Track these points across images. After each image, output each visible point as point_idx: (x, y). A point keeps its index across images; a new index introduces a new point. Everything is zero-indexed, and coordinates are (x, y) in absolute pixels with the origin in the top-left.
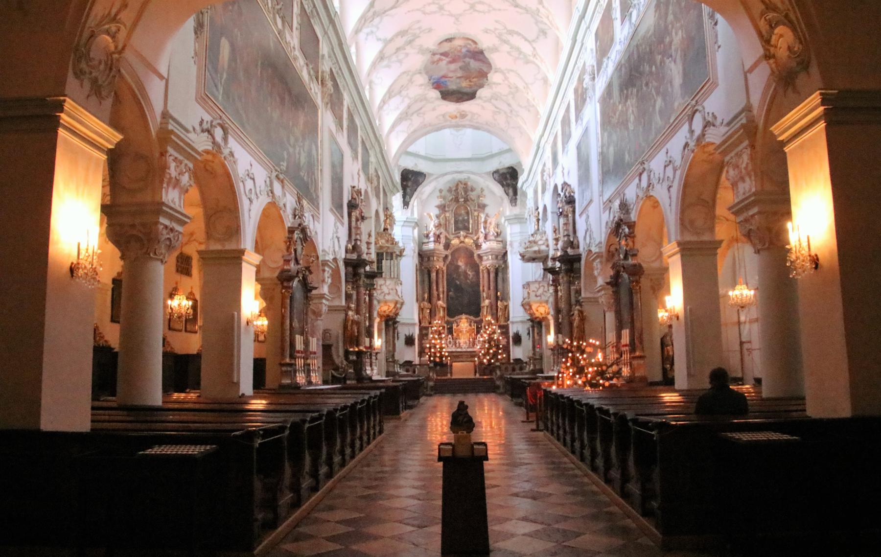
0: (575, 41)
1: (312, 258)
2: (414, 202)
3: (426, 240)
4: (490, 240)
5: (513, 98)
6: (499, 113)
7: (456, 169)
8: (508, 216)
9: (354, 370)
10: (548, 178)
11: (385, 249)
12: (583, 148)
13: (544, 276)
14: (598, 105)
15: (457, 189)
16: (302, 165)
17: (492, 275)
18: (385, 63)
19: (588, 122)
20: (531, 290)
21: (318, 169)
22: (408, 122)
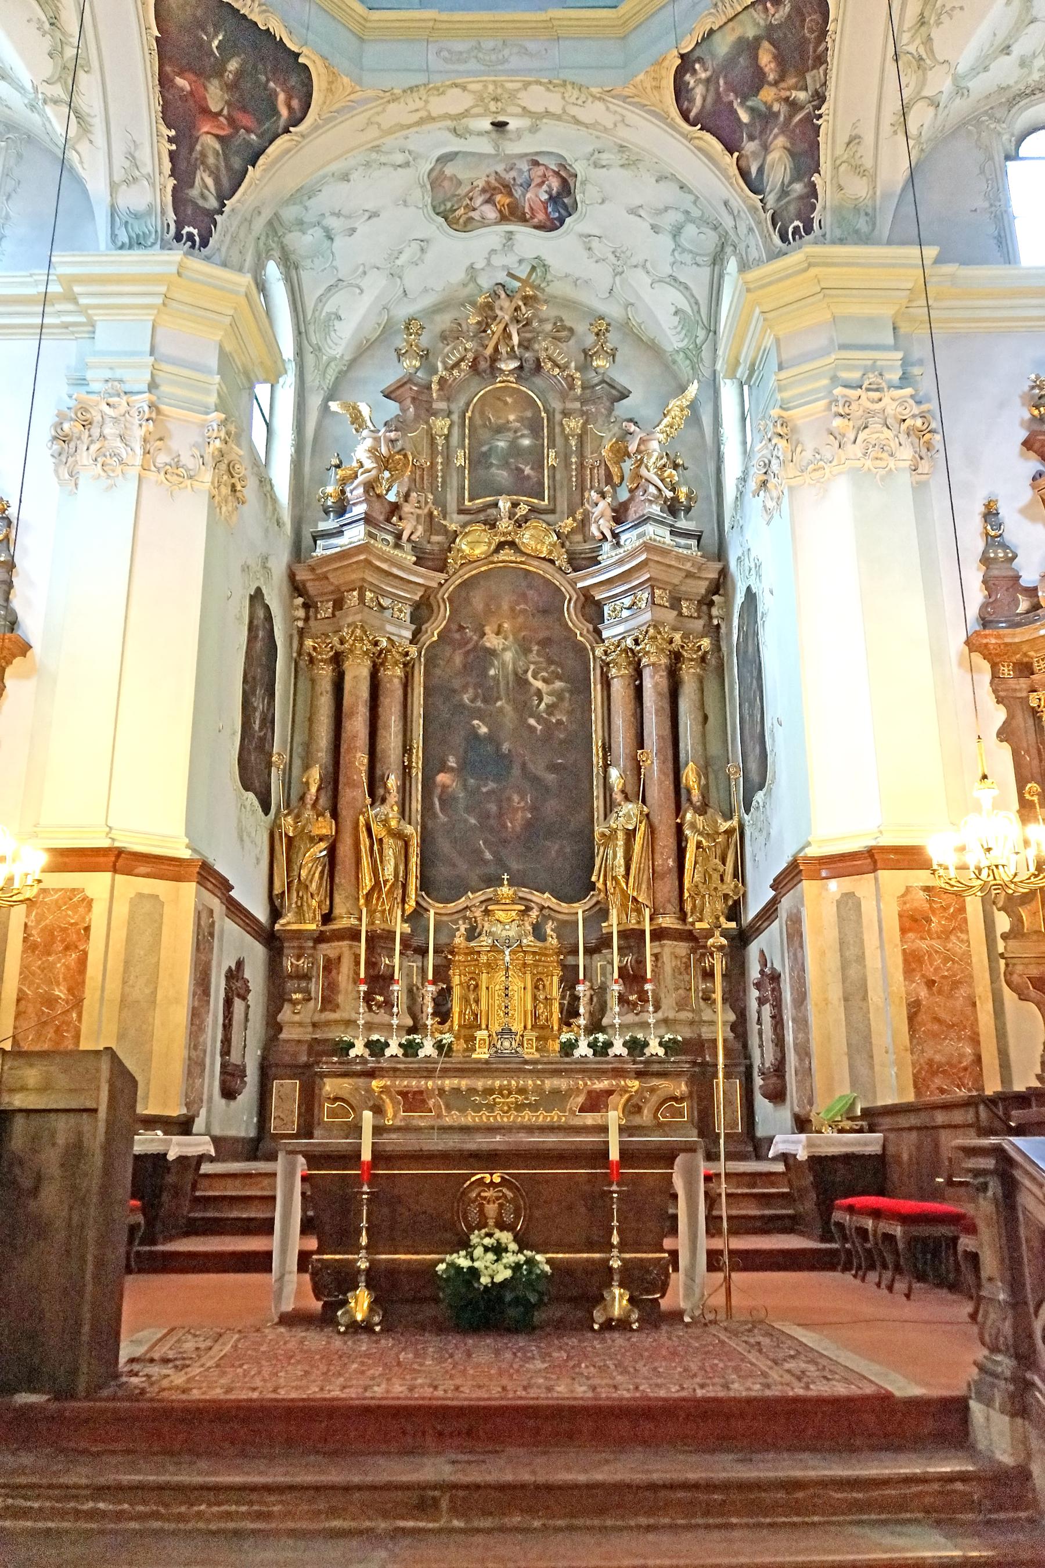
4: (645, 520)
17: (653, 683)
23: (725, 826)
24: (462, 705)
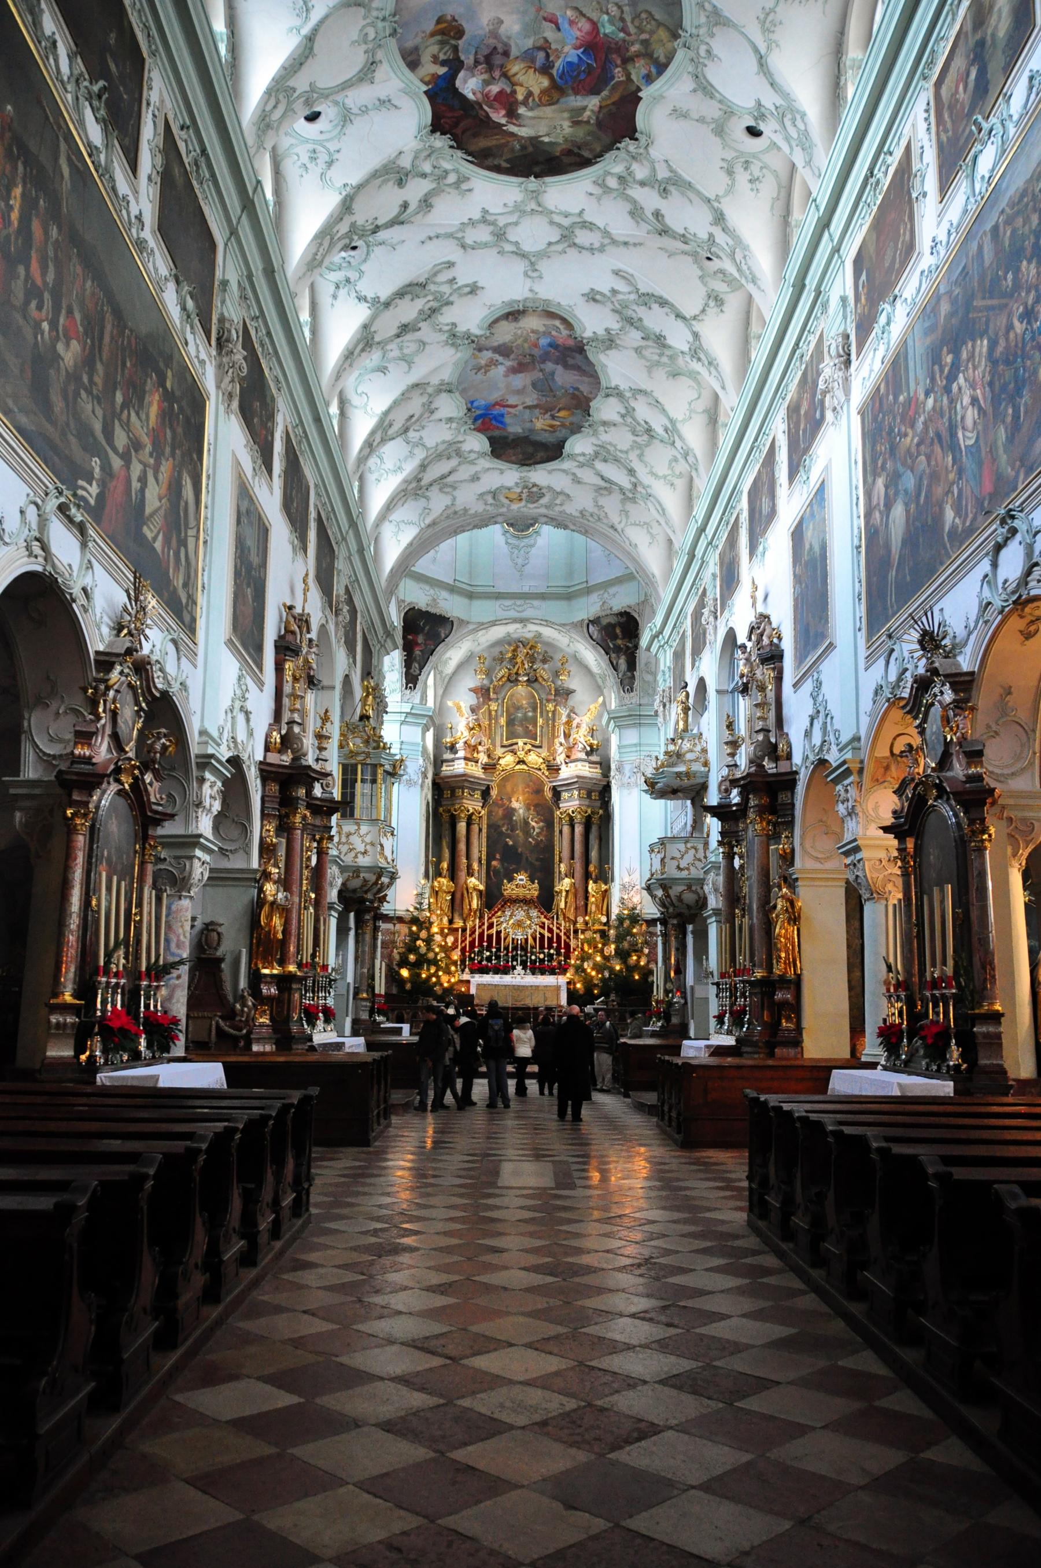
0: (800, 287)
1: (163, 740)
2: (429, 680)
3: (448, 756)
5: (640, 456)
6: (609, 491)
7: (513, 614)
8: (614, 711)
9: (271, 1020)
10: (712, 619)
11: (360, 758)
12: (810, 535)
13: (697, 824)
14: (856, 421)
15: (514, 657)
16: (148, 510)
17: (579, 829)
18: (375, 357)
19: (827, 469)
20: (668, 856)
21: (197, 538)
22: (422, 502)
23: (604, 887)
24: (502, 833)
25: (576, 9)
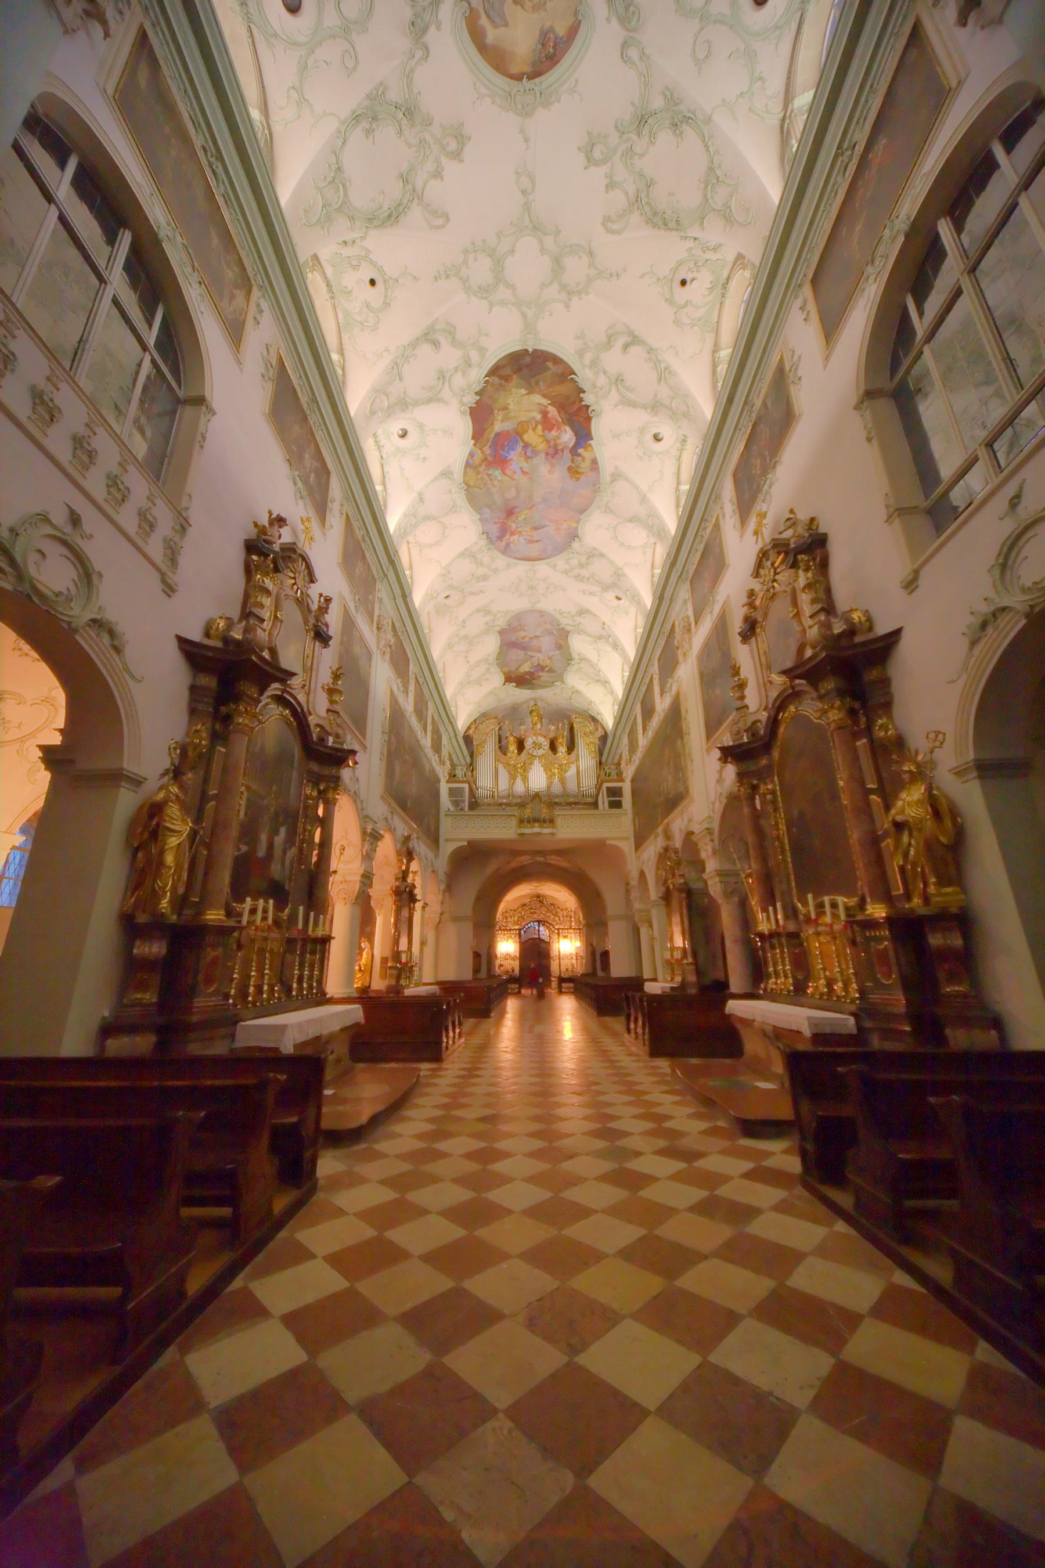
25: (514, 480)
